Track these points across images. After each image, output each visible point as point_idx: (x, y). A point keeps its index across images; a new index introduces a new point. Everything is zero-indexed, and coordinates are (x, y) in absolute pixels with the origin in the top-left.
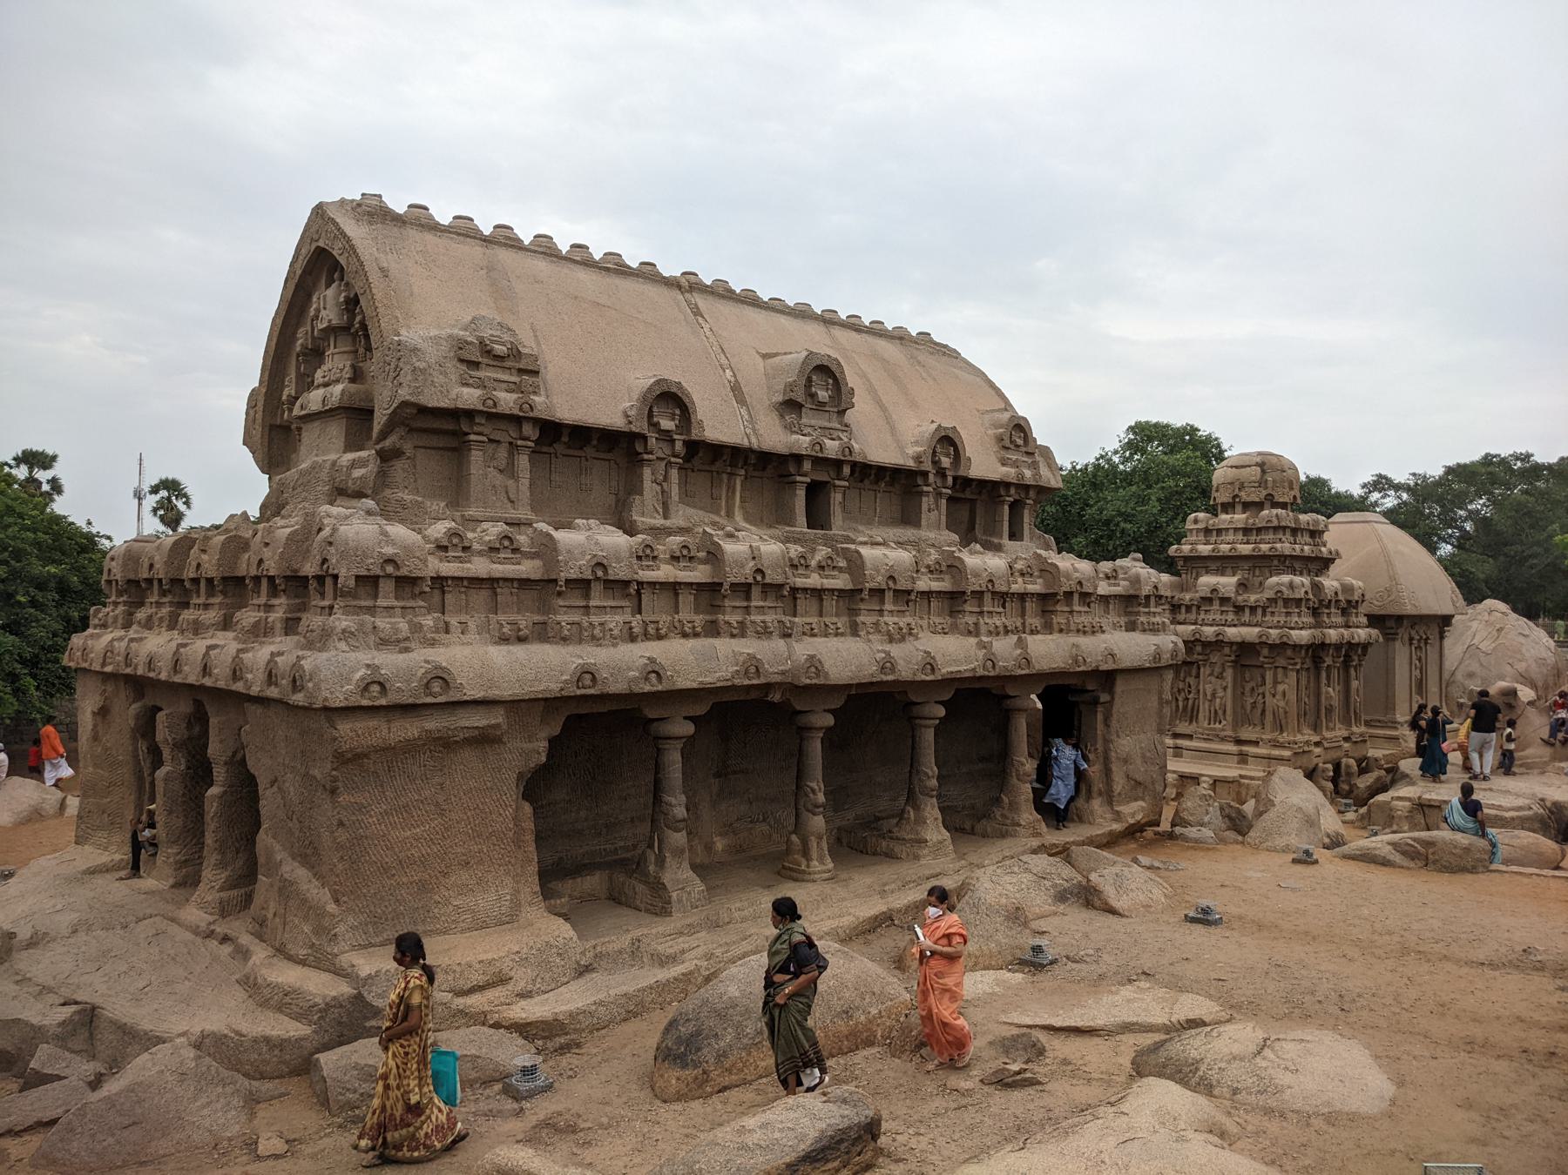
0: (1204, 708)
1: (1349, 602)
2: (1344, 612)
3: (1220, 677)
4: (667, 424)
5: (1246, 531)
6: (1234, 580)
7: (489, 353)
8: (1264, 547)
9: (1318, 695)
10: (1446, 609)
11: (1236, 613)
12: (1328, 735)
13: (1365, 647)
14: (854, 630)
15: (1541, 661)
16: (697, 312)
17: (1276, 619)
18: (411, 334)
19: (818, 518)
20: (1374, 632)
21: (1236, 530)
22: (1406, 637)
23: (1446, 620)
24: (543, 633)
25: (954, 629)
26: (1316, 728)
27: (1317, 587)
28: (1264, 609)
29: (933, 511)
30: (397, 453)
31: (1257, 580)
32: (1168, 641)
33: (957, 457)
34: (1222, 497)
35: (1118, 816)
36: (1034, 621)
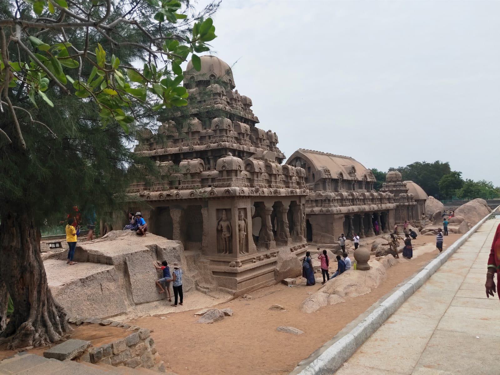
2: (411, 200)
4: (341, 178)
5: (394, 186)
6: (393, 195)
7: (327, 171)
9: (408, 214)
10: (425, 198)
13: (415, 205)
14: (365, 204)
15: (441, 208)
16: (332, 160)
18: (320, 169)
19: (354, 190)
20: (416, 203)
23: (425, 200)
24: (342, 206)
25: (373, 204)
27: (407, 195)
29: (364, 187)
30: (318, 184)
32: (395, 204)
33: (366, 178)
34: (389, 180)
35: (391, 232)
36: (380, 202)
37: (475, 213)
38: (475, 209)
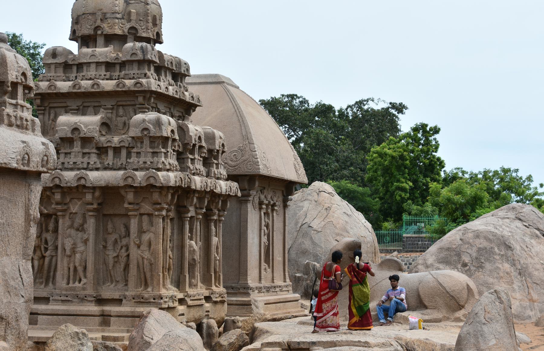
0: (62, 265)
1: (210, 151)
2: (206, 163)
3: (81, 229)
5: (109, 66)
8: (129, 83)
9: (181, 247)
11: (99, 155)
12: (191, 291)
13: (226, 198)
17: (142, 160)
21: (98, 64)
22: (257, 201)
26: (179, 284)
28: (129, 150)
31: (121, 120)
37: (507, 266)
38: (509, 247)
